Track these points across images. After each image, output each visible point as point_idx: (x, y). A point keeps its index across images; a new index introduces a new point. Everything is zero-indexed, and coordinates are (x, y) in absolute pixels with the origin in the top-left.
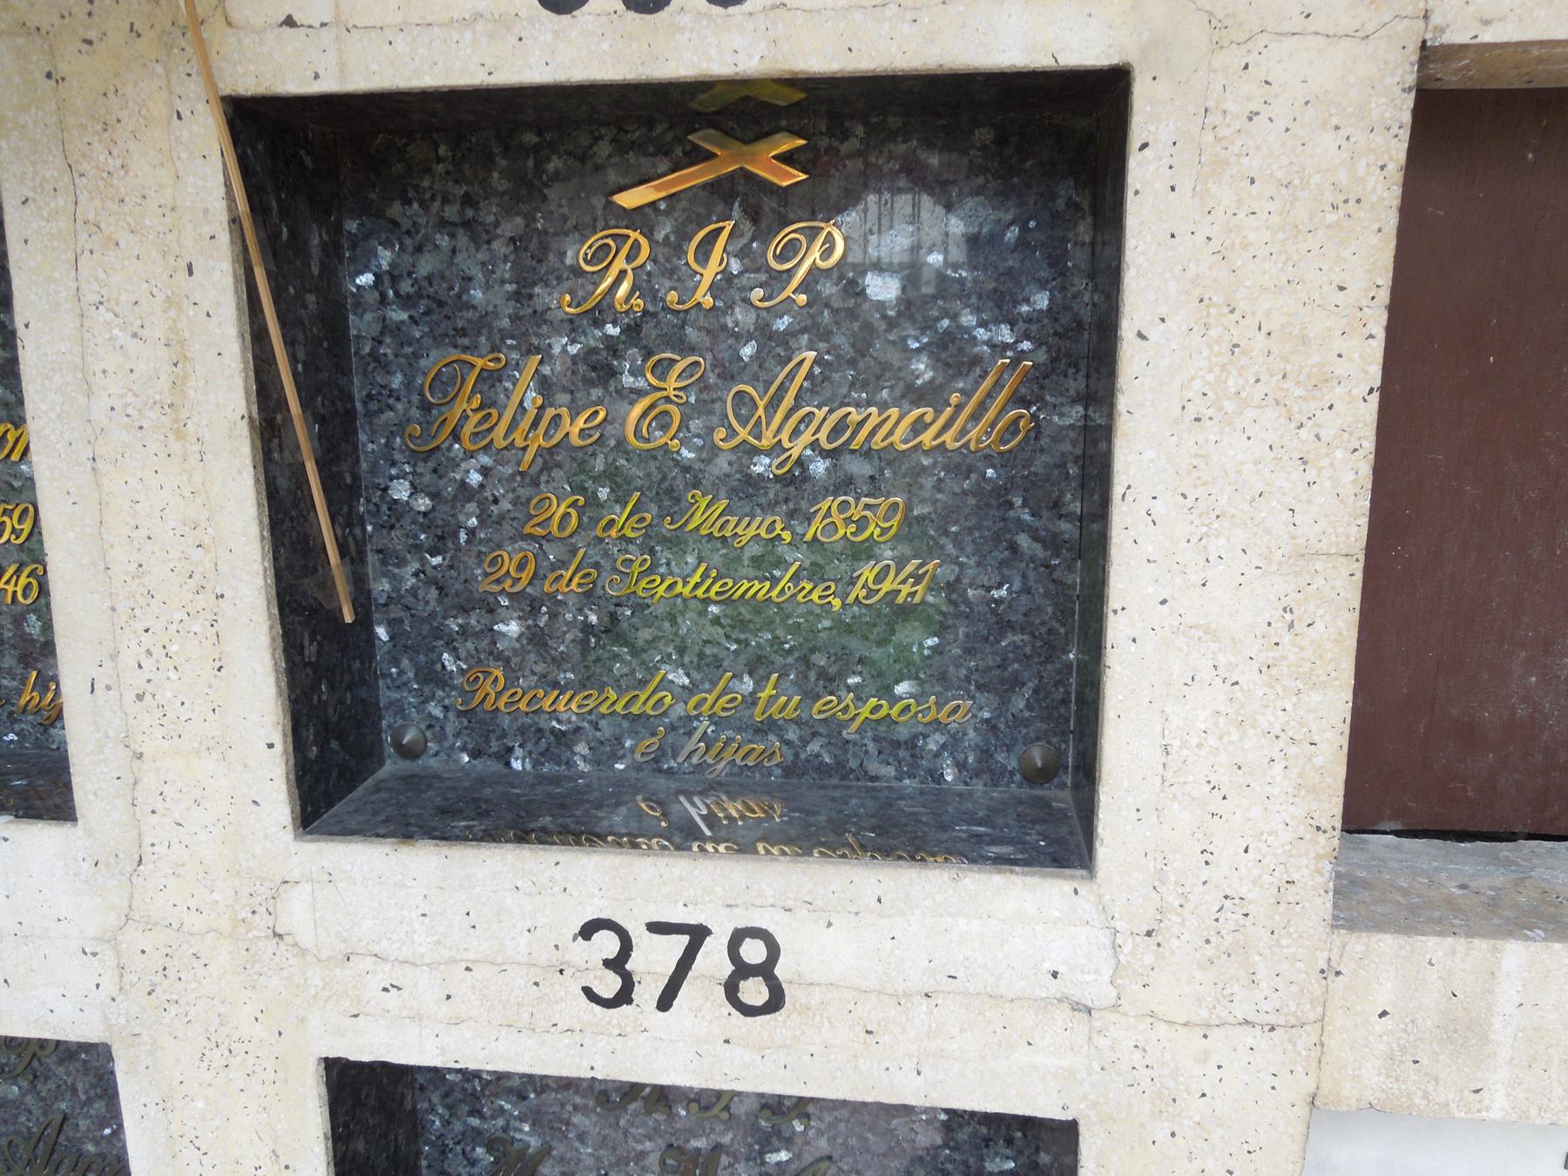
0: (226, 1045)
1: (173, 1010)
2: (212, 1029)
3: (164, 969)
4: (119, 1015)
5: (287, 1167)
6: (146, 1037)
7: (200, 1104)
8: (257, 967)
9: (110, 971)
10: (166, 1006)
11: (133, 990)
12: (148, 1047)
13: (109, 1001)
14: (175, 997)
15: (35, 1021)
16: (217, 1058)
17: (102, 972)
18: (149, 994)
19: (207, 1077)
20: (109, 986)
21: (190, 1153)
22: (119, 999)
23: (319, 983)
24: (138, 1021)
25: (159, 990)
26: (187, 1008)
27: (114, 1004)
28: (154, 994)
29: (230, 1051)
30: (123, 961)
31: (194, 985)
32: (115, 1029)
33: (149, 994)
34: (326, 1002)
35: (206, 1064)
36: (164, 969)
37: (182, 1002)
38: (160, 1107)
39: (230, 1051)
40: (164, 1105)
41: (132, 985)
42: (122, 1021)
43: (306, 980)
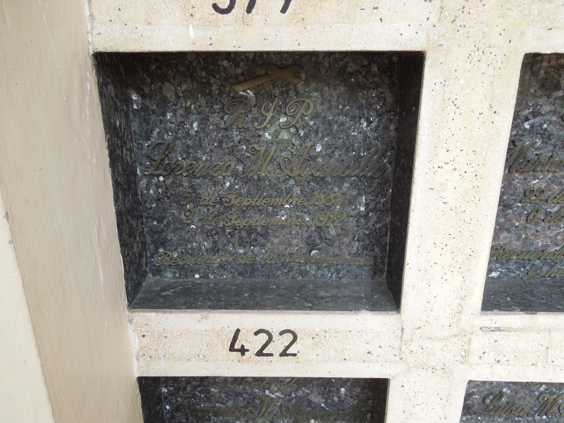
0: (482, 49)
1: (462, 30)
2: (478, 41)
3: (463, 8)
4: (435, 34)
5: (495, 112)
6: (445, 47)
7: (462, 82)
8: (508, 6)
9: (436, 10)
10: (459, 29)
11: (445, 20)
12: (445, 52)
13: (431, 27)
14: (464, 23)
15: (392, 40)
16: (476, 56)
17: (431, 11)
18: (452, 22)
19: (469, 66)
20: (434, 19)
21: (452, 108)
22: (437, 26)
23: (536, 12)
24: (443, 38)
25: (458, 19)
26: (469, 29)
27: (434, 28)
28: (455, 22)
29: (483, 52)
30: (444, 4)
31: (475, 16)
32: (431, 42)
33: (452, 22)
34: (537, 22)
35: (469, 60)
36: (463, 8)
37: (467, 26)
38: (442, 84)
39: (483, 52)
40: (444, 84)
41: (445, 17)
42: (436, 38)
43: (530, 12)
